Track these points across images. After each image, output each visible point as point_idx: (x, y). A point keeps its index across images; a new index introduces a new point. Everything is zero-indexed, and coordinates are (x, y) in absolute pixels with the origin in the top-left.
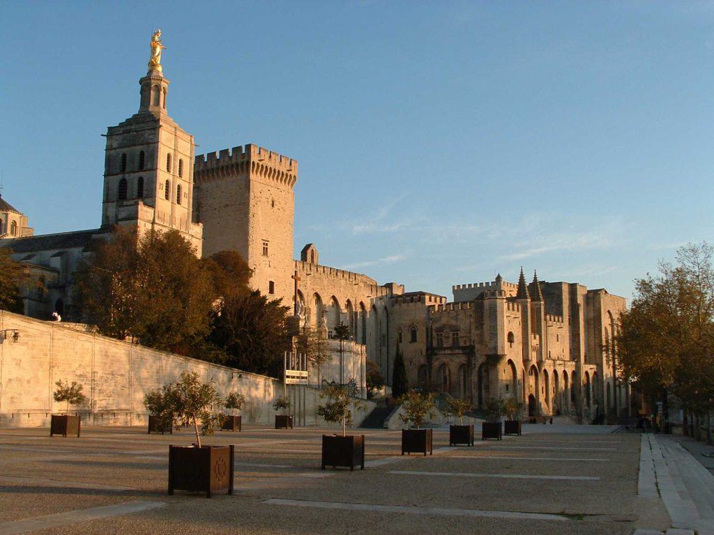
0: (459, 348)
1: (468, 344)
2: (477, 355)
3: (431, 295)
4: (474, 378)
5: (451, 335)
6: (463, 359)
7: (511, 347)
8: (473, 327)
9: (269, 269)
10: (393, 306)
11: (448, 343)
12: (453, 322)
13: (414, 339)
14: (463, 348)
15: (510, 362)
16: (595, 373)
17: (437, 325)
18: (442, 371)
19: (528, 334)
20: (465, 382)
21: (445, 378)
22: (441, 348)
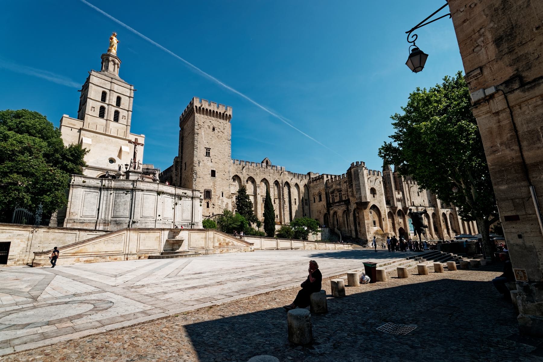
0: (343, 201)
1: (347, 198)
2: (352, 204)
3: (327, 176)
4: (351, 218)
5: (338, 194)
6: (344, 208)
7: (374, 197)
8: (348, 187)
9: (211, 163)
10: (310, 183)
11: (337, 199)
12: (338, 187)
13: (320, 200)
14: (345, 201)
15: (374, 207)
16: (450, 213)
17: (331, 190)
18: (335, 216)
19: (392, 191)
20: (347, 221)
21: (337, 220)
22: (334, 203)
